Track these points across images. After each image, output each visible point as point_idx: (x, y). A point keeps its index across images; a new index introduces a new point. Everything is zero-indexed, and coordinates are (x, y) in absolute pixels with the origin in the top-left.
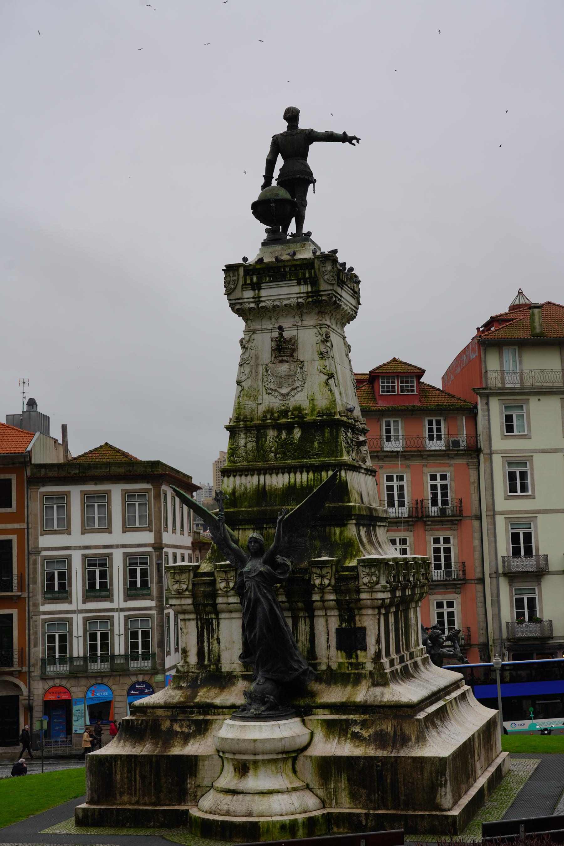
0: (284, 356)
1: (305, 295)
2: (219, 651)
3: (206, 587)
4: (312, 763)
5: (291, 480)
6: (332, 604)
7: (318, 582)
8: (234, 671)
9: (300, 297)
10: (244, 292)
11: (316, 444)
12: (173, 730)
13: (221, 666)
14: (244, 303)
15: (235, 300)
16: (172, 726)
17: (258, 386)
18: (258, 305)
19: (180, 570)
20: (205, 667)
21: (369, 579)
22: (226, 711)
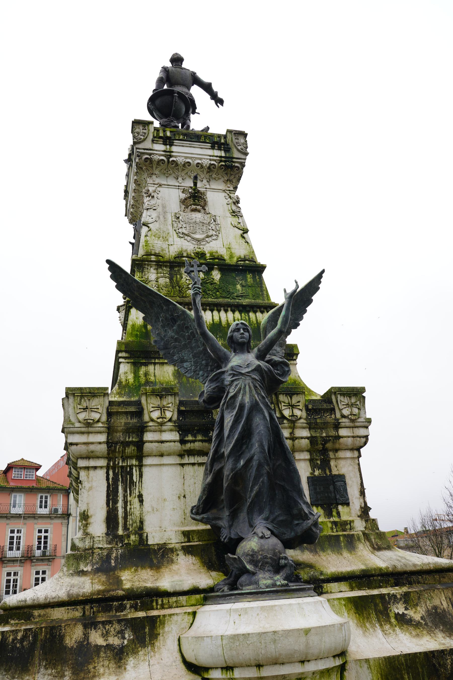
0: (198, 205)
1: (218, 158)
2: (141, 514)
3: (127, 418)
4: (372, 673)
5: (214, 318)
6: (305, 443)
7: (287, 413)
8: (168, 542)
10: (155, 145)
11: (239, 287)
12: (88, 643)
13: (147, 536)
14: (153, 154)
15: (144, 149)
16: (86, 636)
17: (168, 230)
18: (168, 159)
19: (90, 393)
20: (121, 538)
21: (350, 410)
22: (183, 599)
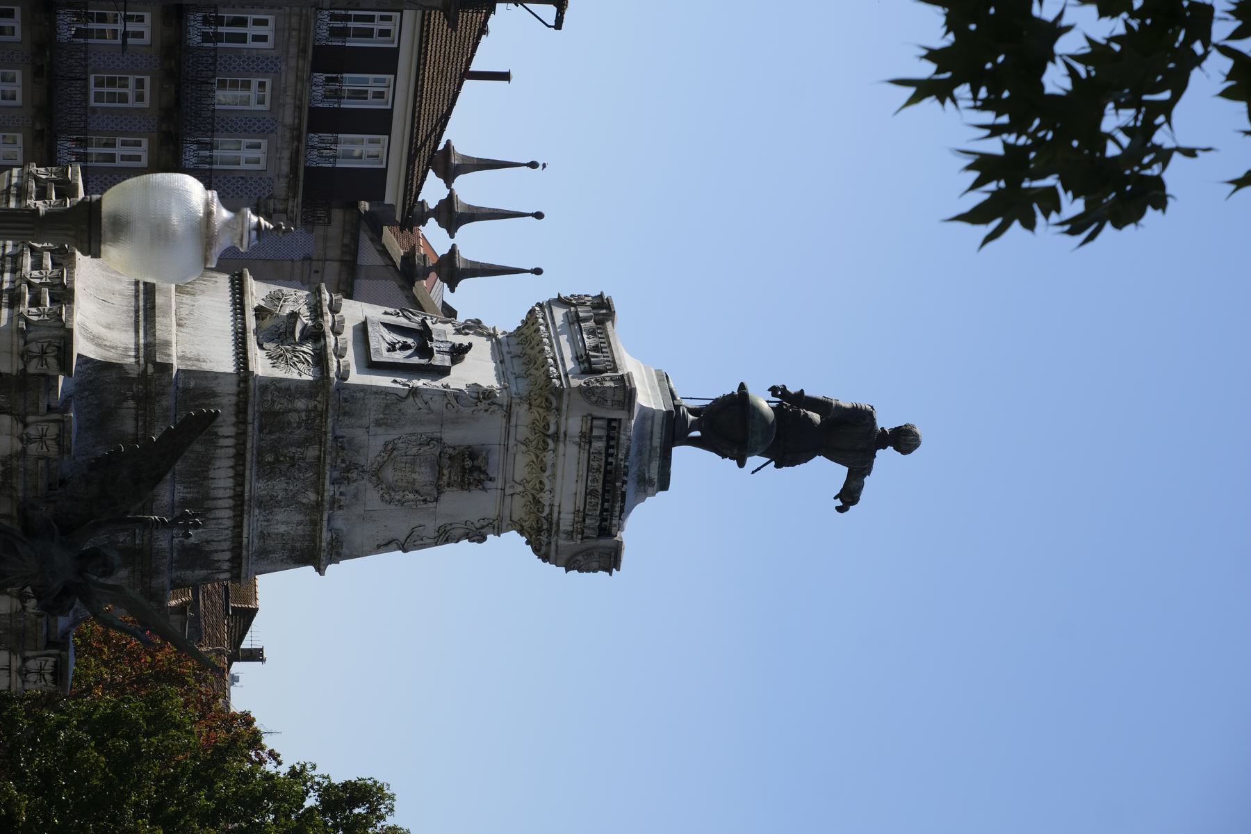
9: (551, 511)
